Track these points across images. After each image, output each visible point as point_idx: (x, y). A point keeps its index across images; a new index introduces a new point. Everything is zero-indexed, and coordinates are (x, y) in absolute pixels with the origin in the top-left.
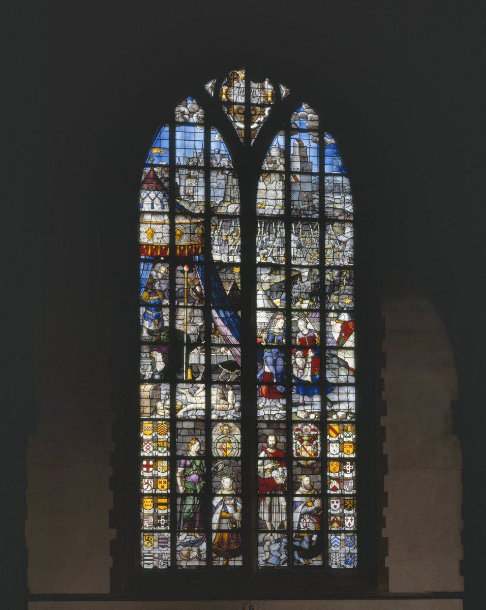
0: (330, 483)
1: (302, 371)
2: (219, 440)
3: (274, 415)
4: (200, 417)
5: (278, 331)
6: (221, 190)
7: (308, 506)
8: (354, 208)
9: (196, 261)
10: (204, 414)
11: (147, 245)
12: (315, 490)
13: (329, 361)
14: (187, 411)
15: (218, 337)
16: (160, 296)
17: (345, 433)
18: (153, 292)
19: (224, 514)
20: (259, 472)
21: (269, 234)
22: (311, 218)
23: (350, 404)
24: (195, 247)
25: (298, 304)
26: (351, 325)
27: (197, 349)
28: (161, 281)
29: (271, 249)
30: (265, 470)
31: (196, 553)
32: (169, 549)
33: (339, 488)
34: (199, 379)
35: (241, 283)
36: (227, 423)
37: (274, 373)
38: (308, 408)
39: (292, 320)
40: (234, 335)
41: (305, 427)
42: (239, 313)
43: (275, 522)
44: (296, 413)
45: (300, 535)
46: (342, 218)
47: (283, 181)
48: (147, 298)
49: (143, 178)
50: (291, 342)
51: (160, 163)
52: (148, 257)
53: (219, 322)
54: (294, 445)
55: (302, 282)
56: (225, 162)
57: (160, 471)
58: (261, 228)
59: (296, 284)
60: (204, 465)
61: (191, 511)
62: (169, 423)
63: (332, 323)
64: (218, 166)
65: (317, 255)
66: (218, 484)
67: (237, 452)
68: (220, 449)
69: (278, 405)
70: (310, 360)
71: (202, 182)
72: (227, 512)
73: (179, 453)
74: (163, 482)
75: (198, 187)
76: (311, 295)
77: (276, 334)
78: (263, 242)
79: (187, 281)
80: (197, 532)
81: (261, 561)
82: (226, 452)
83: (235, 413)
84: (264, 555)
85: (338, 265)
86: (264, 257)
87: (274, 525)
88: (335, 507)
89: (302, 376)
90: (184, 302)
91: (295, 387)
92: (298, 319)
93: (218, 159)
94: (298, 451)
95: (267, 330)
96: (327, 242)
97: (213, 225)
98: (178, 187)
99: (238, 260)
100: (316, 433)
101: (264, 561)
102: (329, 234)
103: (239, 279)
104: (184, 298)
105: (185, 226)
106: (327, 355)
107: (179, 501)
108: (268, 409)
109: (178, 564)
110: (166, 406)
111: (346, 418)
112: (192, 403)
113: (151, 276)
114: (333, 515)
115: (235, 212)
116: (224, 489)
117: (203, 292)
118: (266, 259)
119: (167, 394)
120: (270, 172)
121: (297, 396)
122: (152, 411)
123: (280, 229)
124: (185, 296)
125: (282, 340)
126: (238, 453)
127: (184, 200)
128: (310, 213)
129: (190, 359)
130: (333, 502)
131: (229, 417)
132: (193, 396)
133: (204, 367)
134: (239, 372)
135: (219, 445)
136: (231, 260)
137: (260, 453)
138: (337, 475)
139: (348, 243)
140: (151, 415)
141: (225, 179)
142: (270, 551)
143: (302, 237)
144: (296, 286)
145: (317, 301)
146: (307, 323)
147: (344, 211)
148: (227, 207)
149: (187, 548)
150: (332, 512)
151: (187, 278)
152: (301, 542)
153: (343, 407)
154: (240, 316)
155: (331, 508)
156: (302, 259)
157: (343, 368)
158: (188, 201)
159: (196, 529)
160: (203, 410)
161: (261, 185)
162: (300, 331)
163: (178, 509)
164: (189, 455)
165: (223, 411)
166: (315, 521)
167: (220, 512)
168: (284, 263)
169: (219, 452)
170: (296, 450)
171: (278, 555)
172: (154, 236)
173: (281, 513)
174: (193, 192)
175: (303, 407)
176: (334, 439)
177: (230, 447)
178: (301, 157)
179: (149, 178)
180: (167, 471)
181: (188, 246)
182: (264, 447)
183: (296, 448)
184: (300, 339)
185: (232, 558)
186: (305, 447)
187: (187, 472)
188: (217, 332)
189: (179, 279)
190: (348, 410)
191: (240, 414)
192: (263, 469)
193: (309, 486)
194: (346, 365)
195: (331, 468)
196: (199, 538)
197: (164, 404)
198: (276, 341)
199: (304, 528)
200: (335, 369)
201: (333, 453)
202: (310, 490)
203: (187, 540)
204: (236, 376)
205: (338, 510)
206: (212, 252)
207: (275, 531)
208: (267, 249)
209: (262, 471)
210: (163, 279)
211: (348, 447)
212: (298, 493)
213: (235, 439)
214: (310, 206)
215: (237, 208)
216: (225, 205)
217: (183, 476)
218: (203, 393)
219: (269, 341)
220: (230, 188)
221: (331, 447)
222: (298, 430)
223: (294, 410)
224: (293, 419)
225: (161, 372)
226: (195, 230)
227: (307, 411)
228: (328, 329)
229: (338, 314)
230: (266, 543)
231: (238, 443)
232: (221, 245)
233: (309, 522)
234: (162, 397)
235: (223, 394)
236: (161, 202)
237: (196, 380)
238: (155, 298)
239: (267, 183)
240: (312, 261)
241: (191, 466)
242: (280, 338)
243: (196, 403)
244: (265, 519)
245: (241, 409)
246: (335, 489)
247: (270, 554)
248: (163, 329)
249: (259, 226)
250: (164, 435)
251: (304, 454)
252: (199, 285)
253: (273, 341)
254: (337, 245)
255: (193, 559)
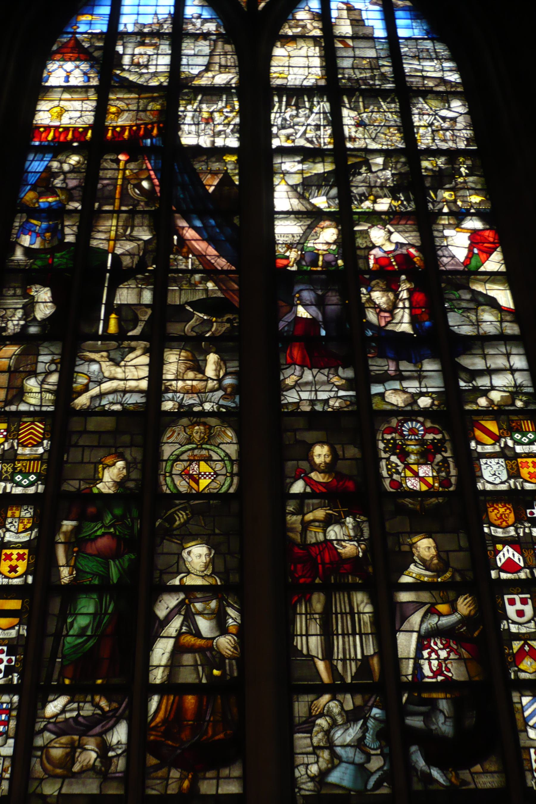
0: (497, 552)
1: (387, 315)
2: (178, 456)
3: (326, 402)
4: (131, 408)
5: (325, 247)
6: (201, 57)
7: (440, 615)
8: (462, 77)
9: (146, 147)
10: (144, 400)
11: (48, 128)
12: (455, 570)
13: (452, 296)
14: (101, 395)
15: (187, 258)
16: (63, 197)
17: (517, 436)
18: (52, 191)
19: (189, 639)
20: (292, 530)
21: (298, 108)
22: (379, 90)
23: (517, 375)
24: (146, 128)
25: (367, 205)
26: (490, 235)
27: (136, 279)
28: (69, 175)
29: (302, 129)
30: (306, 525)
31: (94, 755)
32: (11, 742)
33: (522, 564)
34: (137, 332)
35: (239, 174)
36: (203, 420)
37: (320, 317)
38: (412, 386)
39: (356, 228)
40: (221, 255)
41: (409, 425)
42: (236, 221)
43: (344, 660)
44: (382, 395)
45: (425, 695)
46: (441, 89)
47: (320, 47)
48: (34, 201)
49: (55, 48)
50: (356, 264)
51: (90, 31)
52: (46, 143)
53: (190, 234)
54: (383, 463)
55: (371, 172)
56: (211, 27)
57: (12, 529)
58: (280, 102)
59: (360, 174)
60: (135, 513)
61: (89, 633)
62: (49, 421)
63: (447, 232)
64: (198, 32)
65: (398, 135)
66: (174, 559)
67: (227, 484)
68: (181, 475)
69: (335, 380)
70: (404, 295)
71: (165, 48)
72: (198, 634)
73: (72, 486)
74: (14, 557)
75: (157, 54)
76: (393, 193)
77: (320, 252)
78: (285, 119)
79: (124, 173)
80: (102, 691)
81: (304, 778)
82: (197, 483)
83: (222, 397)
84: (312, 759)
85: (445, 148)
86: (288, 137)
87: (340, 668)
88: (520, 613)
89: (388, 323)
90: (113, 204)
91: (374, 344)
92: (370, 228)
93: (198, 25)
94: (395, 477)
95: (300, 247)
96: (416, 119)
97: (183, 100)
98: (121, 56)
99: (233, 142)
100: (439, 437)
101: (312, 779)
102: (420, 109)
103: (235, 169)
104: (114, 199)
105: (126, 101)
106: (443, 285)
107: (55, 606)
108: (309, 388)
109: (31, 790)
110: (46, 386)
111: (513, 404)
112: (114, 379)
113: (48, 168)
114: (517, 637)
115: (228, 83)
116: (188, 573)
117: (158, 189)
118: (293, 141)
119: (52, 362)
120: (294, 38)
121: (381, 362)
122: (9, 397)
123: (319, 103)
124: (117, 196)
125: (337, 259)
126: (230, 485)
127: (130, 71)
128: (377, 82)
129: (117, 297)
130: (512, 602)
131: (208, 407)
132: (117, 364)
133: (149, 312)
134: (234, 319)
135: (179, 467)
136: (219, 142)
137: (292, 484)
138: (513, 533)
139: (460, 119)
140: (6, 406)
141: (210, 46)
142: (330, 746)
143: (365, 112)
144: (359, 178)
145: (408, 199)
146: (390, 233)
147: (442, 81)
148: (213, 77)
149: (64, 740)
150: (514, 629)
151: (125, 169)
152: (427, 717)
153: (499, 381)
154: (238, 224)
155: (507, 618)
156: (368, 141)
157: (487, 308)
158: (137, 72)
159: (99, 681)
160: (140, 391)
161: (278, 51)
162: (374, 247)
163: (52, 627)
164: (95, 491)
165: (192, 393)
166: (466, 655)
167: (174, 634)
168: (331, 146)
169: (177, 483)
170: (391, 476)
171: (359, 758)
172: (64, 115)
173: (361, 635)
174: (148, 61)
175: (398, 383)
176: (489, 449)
177: (210, 470)
178: (351, 20)
179: (66, 47)
180: (31, 529)
181: (131, 127)
182: (304, 471)
183: (388, 470)
184: (377, 260)
185: (209, 770)
186: (415, 467)
187: (86, 533)
188: (185, 250)
189: (106, 172)
190: (515, 386)
191: (237, 399)
192: (302, 522)
193: (435, 561)
194: (493, 303)
195: (493, 515)
196: (107, 709)
197: (43, 382)
198: (320, 263)
199: (435, 676)
200: (467, 310)
201: (491, 479)
202: (439, 572)
203: (68, 715)
204: (228, 325)
205: (529, 622)
206: (180, 133)
207: (345, 688)
208: (294, 128)
209: (299, 527)
210: (70, 172)
211: (530, 465)
212: (405, 579)
213: (222, 454)
214: (375, 75)
215: (233, 78)
216: (210, 74)
217: (73, 540)
218: (145, 359)
219: (304, 263)
220: (220, 55)
221: (483, 467)
222: (391, 430)
223: (376, 389)
224: (375, 407)
225: (43, 320)
226: (147, 105)
227: (410, 390)
228: (438, 242)
229: (457, 219)
230: (319, 721)
231: (230, 460)
232: (198, 124)
233: (446, 659)
234: (41, 368)
235: (194, 360)
236: (85, 74)
237: (130, 334)
238: (50, 199)
239: (289, 49)
240: (389, 143)
241: (98, 518)
242: (330, 258)
243: (125, 380)
244: (314, 653)
245: (236, 390)
246: (510, 566)
247: (334, 755)
248: (64, 246)
249: (276, 99)
250: (34, 446)
251: (412, 484)
252: (149, 179)
253: (314, 263)
254: (438, 121)
255: (82, 771)
